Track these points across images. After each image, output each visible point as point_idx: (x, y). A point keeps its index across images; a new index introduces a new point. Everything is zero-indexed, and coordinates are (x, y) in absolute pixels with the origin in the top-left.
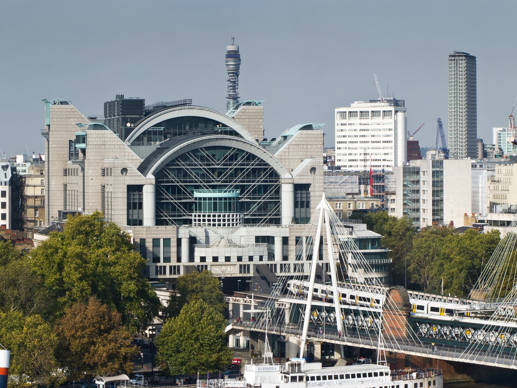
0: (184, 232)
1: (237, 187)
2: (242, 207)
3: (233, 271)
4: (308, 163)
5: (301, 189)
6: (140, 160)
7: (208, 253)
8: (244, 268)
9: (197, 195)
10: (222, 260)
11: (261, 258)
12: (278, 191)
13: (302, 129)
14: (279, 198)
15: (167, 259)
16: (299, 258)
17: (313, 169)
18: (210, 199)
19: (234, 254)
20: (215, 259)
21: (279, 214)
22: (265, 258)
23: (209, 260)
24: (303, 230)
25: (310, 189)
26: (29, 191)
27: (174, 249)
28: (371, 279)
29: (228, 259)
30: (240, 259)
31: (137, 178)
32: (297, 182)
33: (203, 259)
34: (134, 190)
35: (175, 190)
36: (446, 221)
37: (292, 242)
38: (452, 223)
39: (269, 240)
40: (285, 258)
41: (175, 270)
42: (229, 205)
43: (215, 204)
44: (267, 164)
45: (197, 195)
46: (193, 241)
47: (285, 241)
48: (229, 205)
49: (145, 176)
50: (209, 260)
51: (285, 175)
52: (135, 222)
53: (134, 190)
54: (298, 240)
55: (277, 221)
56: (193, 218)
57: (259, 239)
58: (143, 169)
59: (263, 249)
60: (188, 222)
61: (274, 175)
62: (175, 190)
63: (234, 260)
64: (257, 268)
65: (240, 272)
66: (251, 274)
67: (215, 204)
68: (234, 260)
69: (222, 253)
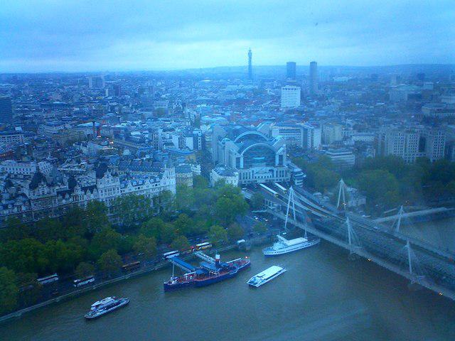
2: (264, 161)
3: (264, 181)
4: (282, 149)
5: (281, 157)
7: (257, 175)
12: (274, 157)
24: (281, 169)
26: (207, 140)
31: (238, 156)
34: (238, 159)
36: (315, 146)
39: (272, 171)
40: (277, 176)
42: (262, 161)
47: (277, 172)
48: (262, 161)
52: (238, 167)
53: (238, 159)
55: (274, 165)
58: (240, 152)
60: (251, 166)
64: (270, 181)
69: (260, 175)
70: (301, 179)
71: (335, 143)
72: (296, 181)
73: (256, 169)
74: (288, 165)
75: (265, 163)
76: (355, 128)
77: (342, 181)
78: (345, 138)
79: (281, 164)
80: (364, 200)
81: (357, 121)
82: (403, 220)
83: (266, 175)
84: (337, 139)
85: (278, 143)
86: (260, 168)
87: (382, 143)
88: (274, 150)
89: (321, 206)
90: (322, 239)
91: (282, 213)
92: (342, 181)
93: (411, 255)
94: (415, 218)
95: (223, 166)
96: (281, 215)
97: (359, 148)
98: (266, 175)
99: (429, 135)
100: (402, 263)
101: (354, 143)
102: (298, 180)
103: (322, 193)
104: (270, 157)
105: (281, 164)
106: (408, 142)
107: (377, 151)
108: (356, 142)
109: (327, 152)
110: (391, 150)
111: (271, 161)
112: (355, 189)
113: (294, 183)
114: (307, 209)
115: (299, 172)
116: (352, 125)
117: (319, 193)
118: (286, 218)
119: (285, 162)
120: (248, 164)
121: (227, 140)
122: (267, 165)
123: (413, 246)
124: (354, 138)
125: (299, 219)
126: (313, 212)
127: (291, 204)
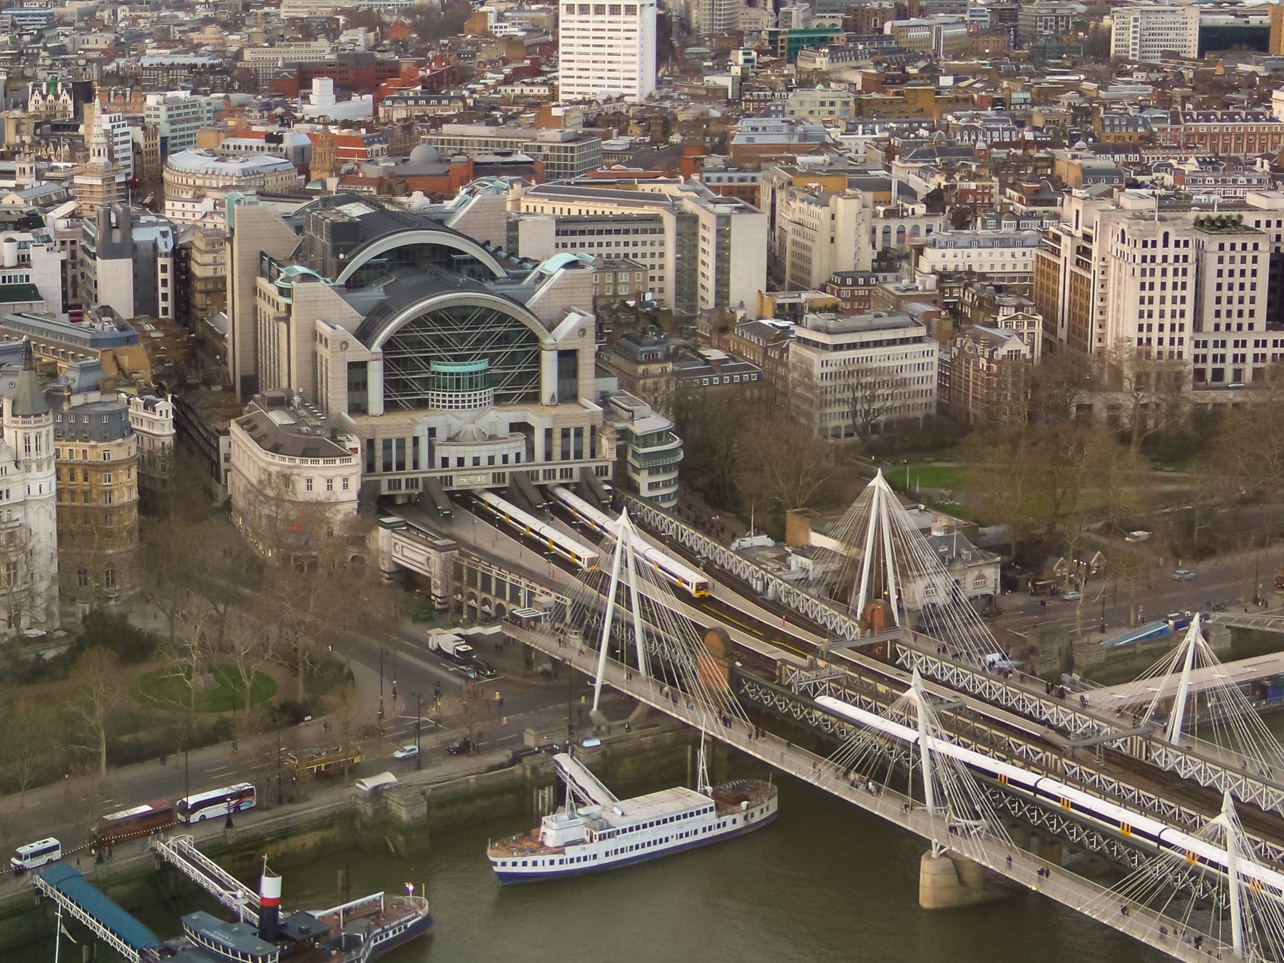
0: (419, 423)
1: (484, 356)
2: (490, 380)
5: (568, 358)
6: (357, 319)
7: (452, 453)
8: (498, 477)
9: (436, 367)
10: (468, 462)
11: (518, 455)
12: (537, 359)
13: (569, 265)
14: (539, 366)
15: (401, 466)
16: (565, 455)
17: (583, 332)
18: (451, 374)
19: (483, 452)
20: (461, 461)
21: (538, 385)
22: (523, 457)
23: (453, 463)
25: (580, 355)
27: (409, 451)
28: (657, 484)
29: (476, 461)
30: (491, 460)
32: (561, 348)
33: (445, 462)
35: (404, 363)
36: (734, 300)
37: (557, 436)
38: (742, 305)
40: (548, 456)
41: (412, 483)
42: (473, 382)
43: (458, 380)
44: (524, 326)
45: (436, 367)
46: (432, 432)
47: (549, 433)
48: (473, 382)
49: (369, 348)
50: (453, 463)
51: (548, 340)
54: (565, 434)
55: (534, 398)
56: (430, 397)
57: (517, 427)
59: (519, 445)
60: (422, 404)
61: (533, 338)
62: (404, 363)
63: (484, 462)
65: (494, 482)
66: (507, 485)
67: (458, 380)
68: (484, 462)
69: (469, 453)
70: (667, 469)
71: (840, 280)
72: (643, 480)
73: (443, 417)
74: (603, 399)
75: (490, 392)
76: (935, 201)
77: (878, 483)
78: (887, 261)
79: (568, 395)
81: (949, 171)
83: (498, 450)
84: (846, 265)
85: (556, 289)
86: (467, 414)
87: (1080, 287)
88: (539, 329)
89: (775, 606)
90: (787, 784)
91: (576, 641)
92: (878, 483)
95: (281, 403)
96: (572, 650)
97: (960, 308)
98: (498, 450)
101: (931, 282)
102: (653, 471)
103: (779, 537)
104: (511, 358)
105: (568, 395)
106: (1211, 280)
107: (1050, 327)
108: (943, 276)
109: (800, 332)
111: (522, 378)
113: (634, 489)
114: (707, 621)
115: (660, 436)
116: (924, 186)
117: (764, 540)
118: (601, 669)
119: (587, 381)
120: (406, 389)
121: (305, 278)
122: (499, 400)
124: (932, 259)
125: (663, 672)
126: (737, 636)
127: (623, 595)
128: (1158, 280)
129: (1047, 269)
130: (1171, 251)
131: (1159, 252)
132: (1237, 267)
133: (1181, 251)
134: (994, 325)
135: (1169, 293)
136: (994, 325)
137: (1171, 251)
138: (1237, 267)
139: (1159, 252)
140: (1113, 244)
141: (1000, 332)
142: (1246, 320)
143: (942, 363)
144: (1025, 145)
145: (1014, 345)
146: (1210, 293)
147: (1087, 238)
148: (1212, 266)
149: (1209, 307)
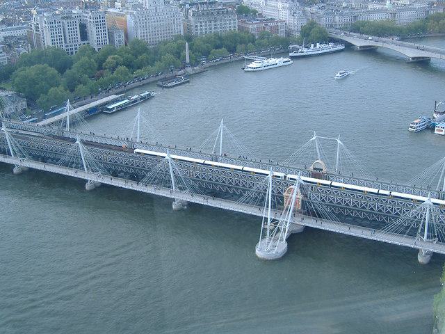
80: (25, 103)
82: (72, 117)
93: (83, 150)
94: (87, 111)
99: (89, 20)
100: (75, 163)
106: (67, 31)
110: (48, 41)
112: (11, 92)
123: (86, 143)
128: (55, 32)
129: (30, 33)
130: (57, 25)
131: (54, 25)
132: (72, 27)
133: (59, 24)
134: (19, 47)
135: (58, 35)
136: (19, 47)
137: (57, 25)
138: (72, 27)
139: (54, 25)
140: (44, 25)
141: (21, 49)
142: (76, 40)
143: (8, 59)
144: (23, 8)
145: (24, 51)
146: (67, 34)
147: (38, 24)
148: (66, 28)
149: (68, 38)
